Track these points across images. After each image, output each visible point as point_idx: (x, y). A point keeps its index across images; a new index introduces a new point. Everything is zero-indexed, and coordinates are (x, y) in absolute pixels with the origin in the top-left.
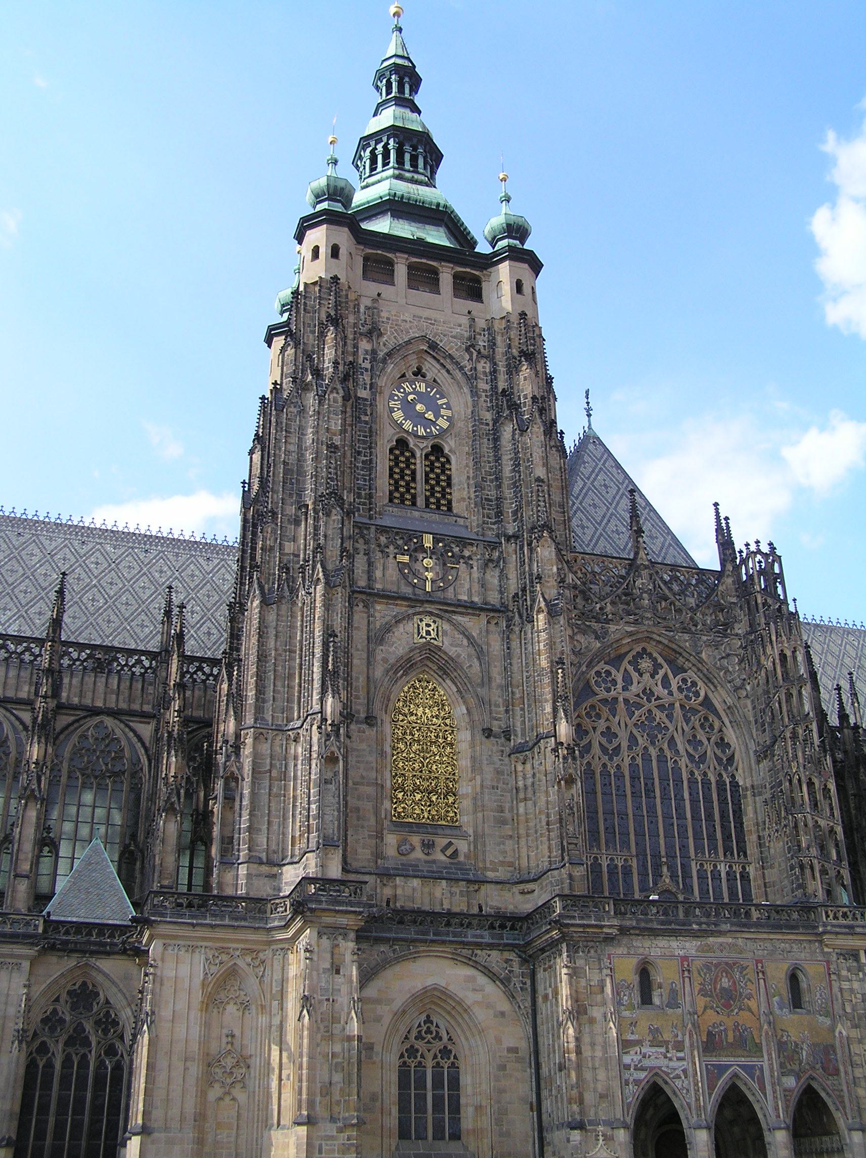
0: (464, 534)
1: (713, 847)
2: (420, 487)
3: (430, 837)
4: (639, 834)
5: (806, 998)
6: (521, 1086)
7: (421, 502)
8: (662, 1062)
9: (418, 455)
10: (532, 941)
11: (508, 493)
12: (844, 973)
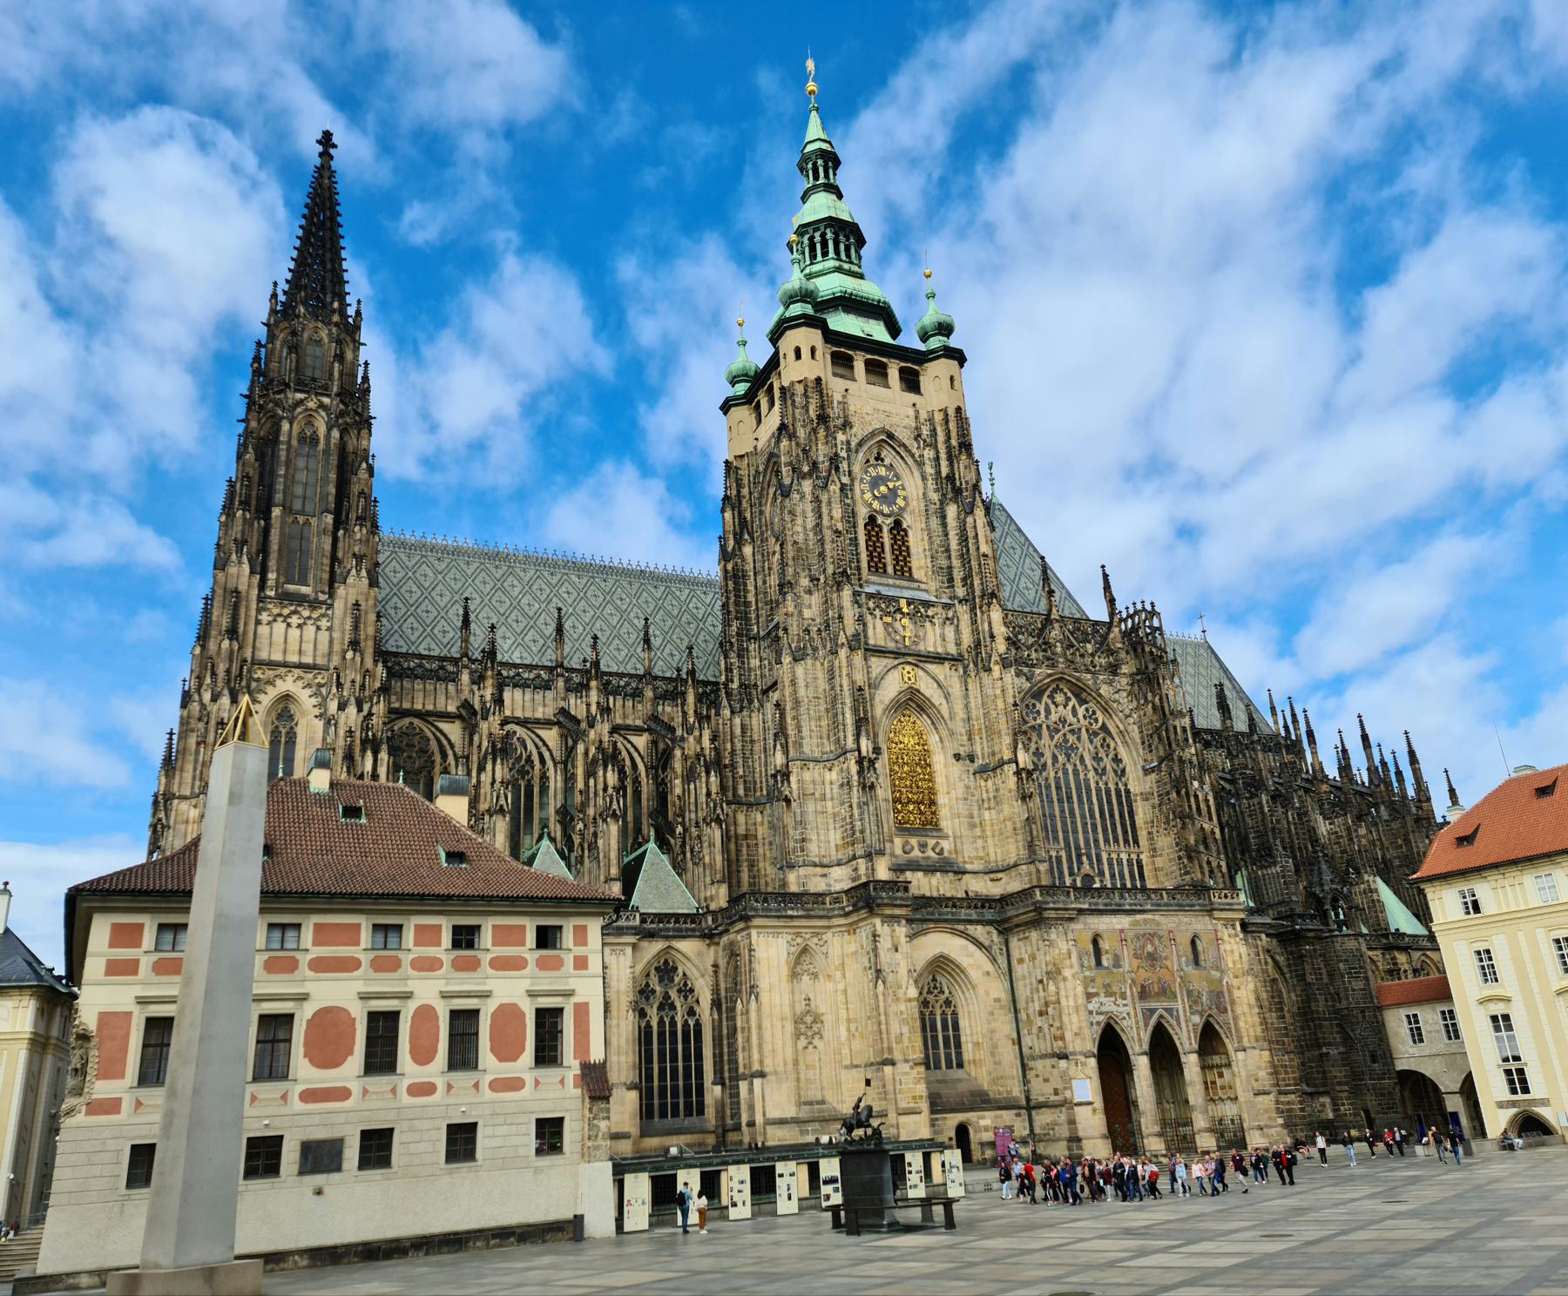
0: (924, 596)
1: (1116, 840)
2: (888, 557)
3: (923, 839)
4: (1065, 832)
5: (1202, 957)
6: (1005, 1027)
7: (890, 570)
8: (1114, 1008)
9: (885, 529)
10: (1010, 918)
11: (956, 563)
12: (1226, 938)
